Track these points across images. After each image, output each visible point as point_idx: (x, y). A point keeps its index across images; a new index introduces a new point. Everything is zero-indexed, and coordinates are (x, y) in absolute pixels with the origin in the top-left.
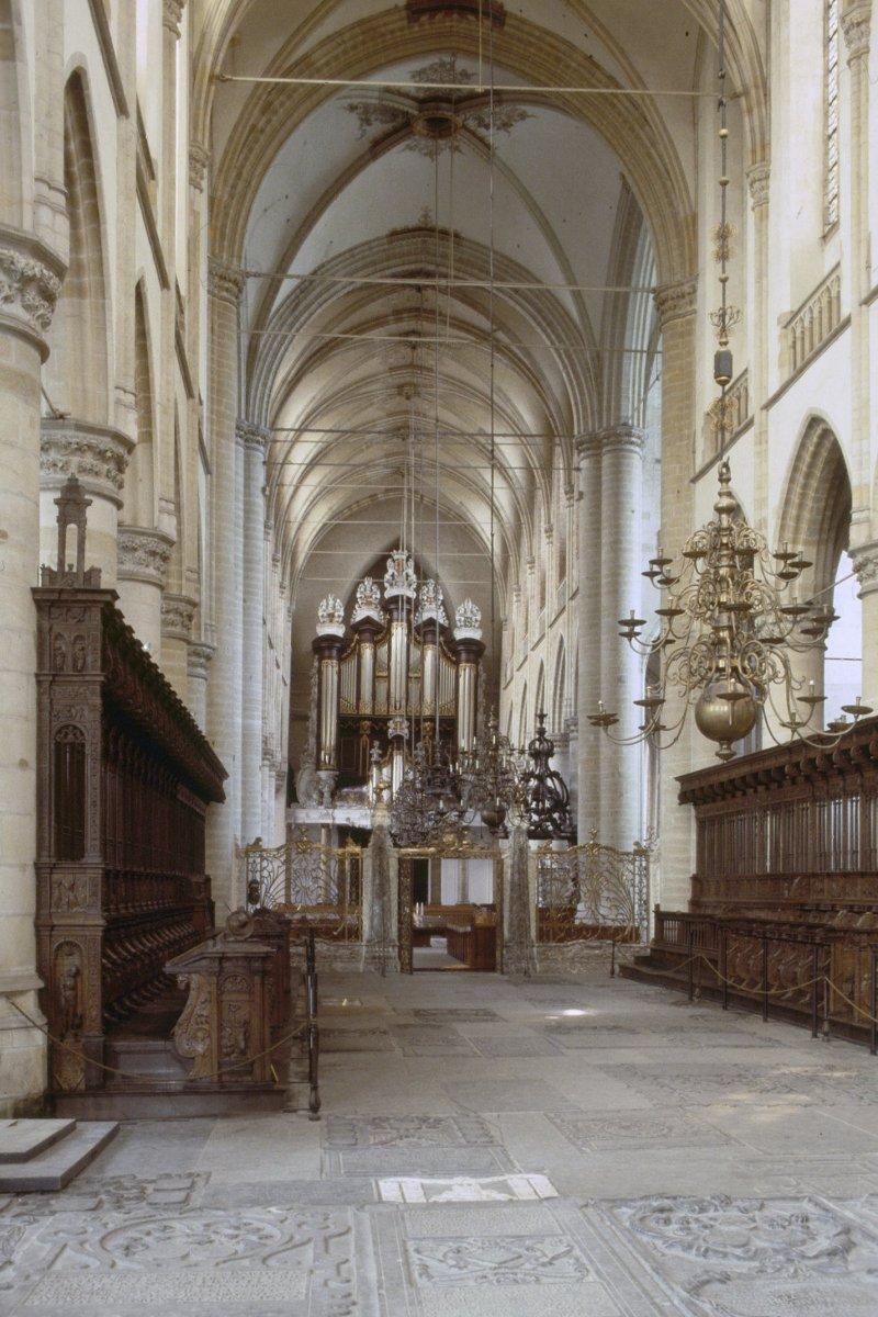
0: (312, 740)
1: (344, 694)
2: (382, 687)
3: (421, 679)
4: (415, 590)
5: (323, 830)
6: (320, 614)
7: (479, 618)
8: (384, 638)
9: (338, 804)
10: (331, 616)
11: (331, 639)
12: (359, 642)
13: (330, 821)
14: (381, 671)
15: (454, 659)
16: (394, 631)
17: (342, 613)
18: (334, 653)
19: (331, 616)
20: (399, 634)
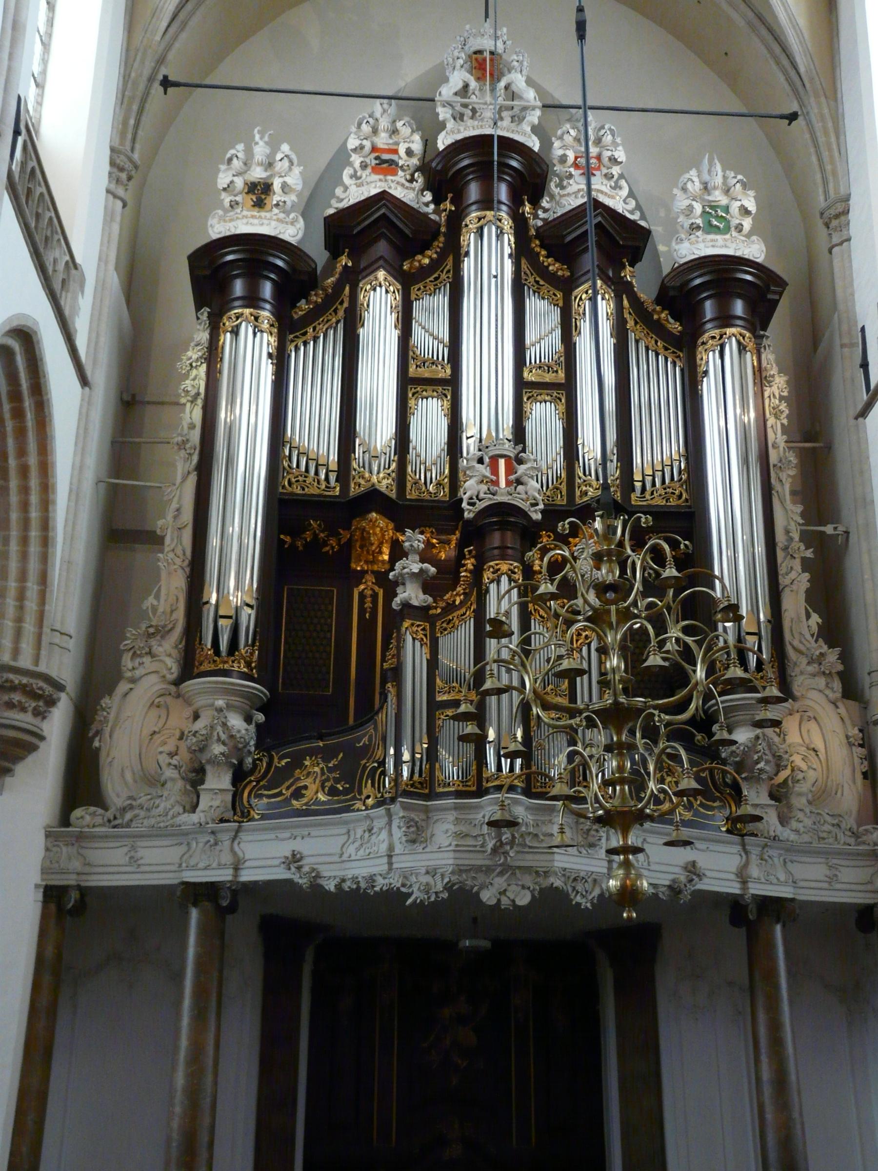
0: (173, 584)
1: (294, 429)
2: (430, 416)
3: (565, 391)
4: (535, 130)
5: (194, 914)
6: (223, 180)
7: (751, 206)
8: (435, 265)
9: (260, 805)
10: (259, 193)
11: (256, 248)
12: (353, 278)
13: (224, 875)
14: (428, 378)
15: (675, 327)
16: (469, 239)
17: (294, 179)
18: (267, 290)
19: (259, 193)
20: (489, 256)
